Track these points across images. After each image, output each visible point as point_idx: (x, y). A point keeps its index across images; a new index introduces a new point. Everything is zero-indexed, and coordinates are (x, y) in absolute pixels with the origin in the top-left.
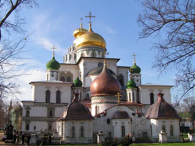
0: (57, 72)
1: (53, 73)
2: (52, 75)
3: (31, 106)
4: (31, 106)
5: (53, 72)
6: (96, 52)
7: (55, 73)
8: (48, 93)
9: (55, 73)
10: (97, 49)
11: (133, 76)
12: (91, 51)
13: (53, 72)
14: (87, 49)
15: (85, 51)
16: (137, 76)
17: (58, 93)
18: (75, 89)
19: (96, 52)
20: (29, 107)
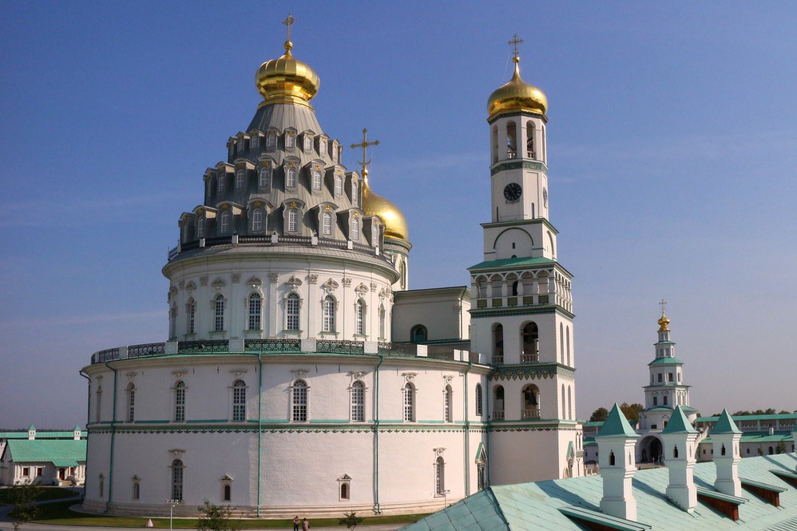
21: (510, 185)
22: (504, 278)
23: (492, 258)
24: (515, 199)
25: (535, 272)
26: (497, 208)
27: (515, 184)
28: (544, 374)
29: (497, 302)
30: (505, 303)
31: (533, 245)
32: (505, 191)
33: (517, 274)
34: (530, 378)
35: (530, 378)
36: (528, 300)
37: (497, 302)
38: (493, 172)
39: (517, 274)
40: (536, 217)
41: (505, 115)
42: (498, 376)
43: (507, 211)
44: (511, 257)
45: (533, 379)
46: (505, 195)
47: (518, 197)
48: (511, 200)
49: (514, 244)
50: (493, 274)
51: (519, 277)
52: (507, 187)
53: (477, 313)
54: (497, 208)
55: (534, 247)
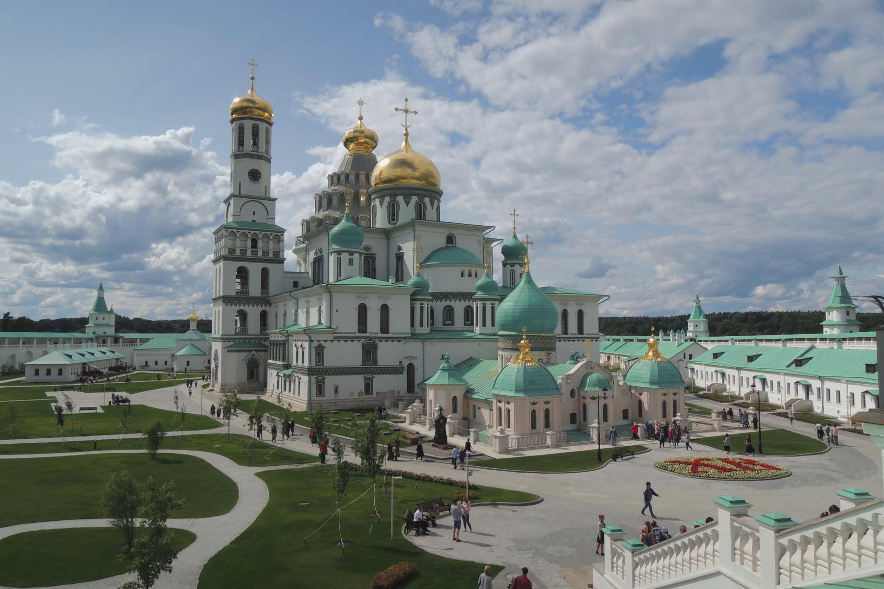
0: (361, 254)
1: (351, 257)
2: (351, 262)
3: (325, 341)
4: (325, 341)
5: (351, 253)
6: (427, 200)
7: (356, 257)
8: (363, 310)
9: (356, 257)
10: (428, 194)
11: (512, 265)
12: (414, 199)
13: (351, 253)
14: (406, 191)
15: (401, 197)
16: (520, 266)
17: (385, 309)
18: (416, 300)
19: (427, 200)
20: (322, 343)
21: (253, 169)
22: (249, 236)
23: (239, 219)
24: (256, 181)
25: (271, 234)
26: (240, 183)
27: (256, 170)
28: (261, 304)
29: (243, 252)
30: (249, 253)
31: (268, 215)
32: (249, 173)
33: (259, 234)
34: (264, 306)
35: (264, 306)
36: (265, 253)
37: (243, 252)
38: (236, 156)
39: (259, 234)
40: (267, 196)
41: (252, 119)
42: (246, 303)
43: (249, 188)
44: (251, 221)
45: (266, 307)
46: (249, 176)
47: (259, 179)
48: (253, 180)
49: (254, 212)
50: (253, 232)
51: (260, 236)
52: (251, 171)
53: (226, 257)
54: (240, 183)
55: (269, 217)
